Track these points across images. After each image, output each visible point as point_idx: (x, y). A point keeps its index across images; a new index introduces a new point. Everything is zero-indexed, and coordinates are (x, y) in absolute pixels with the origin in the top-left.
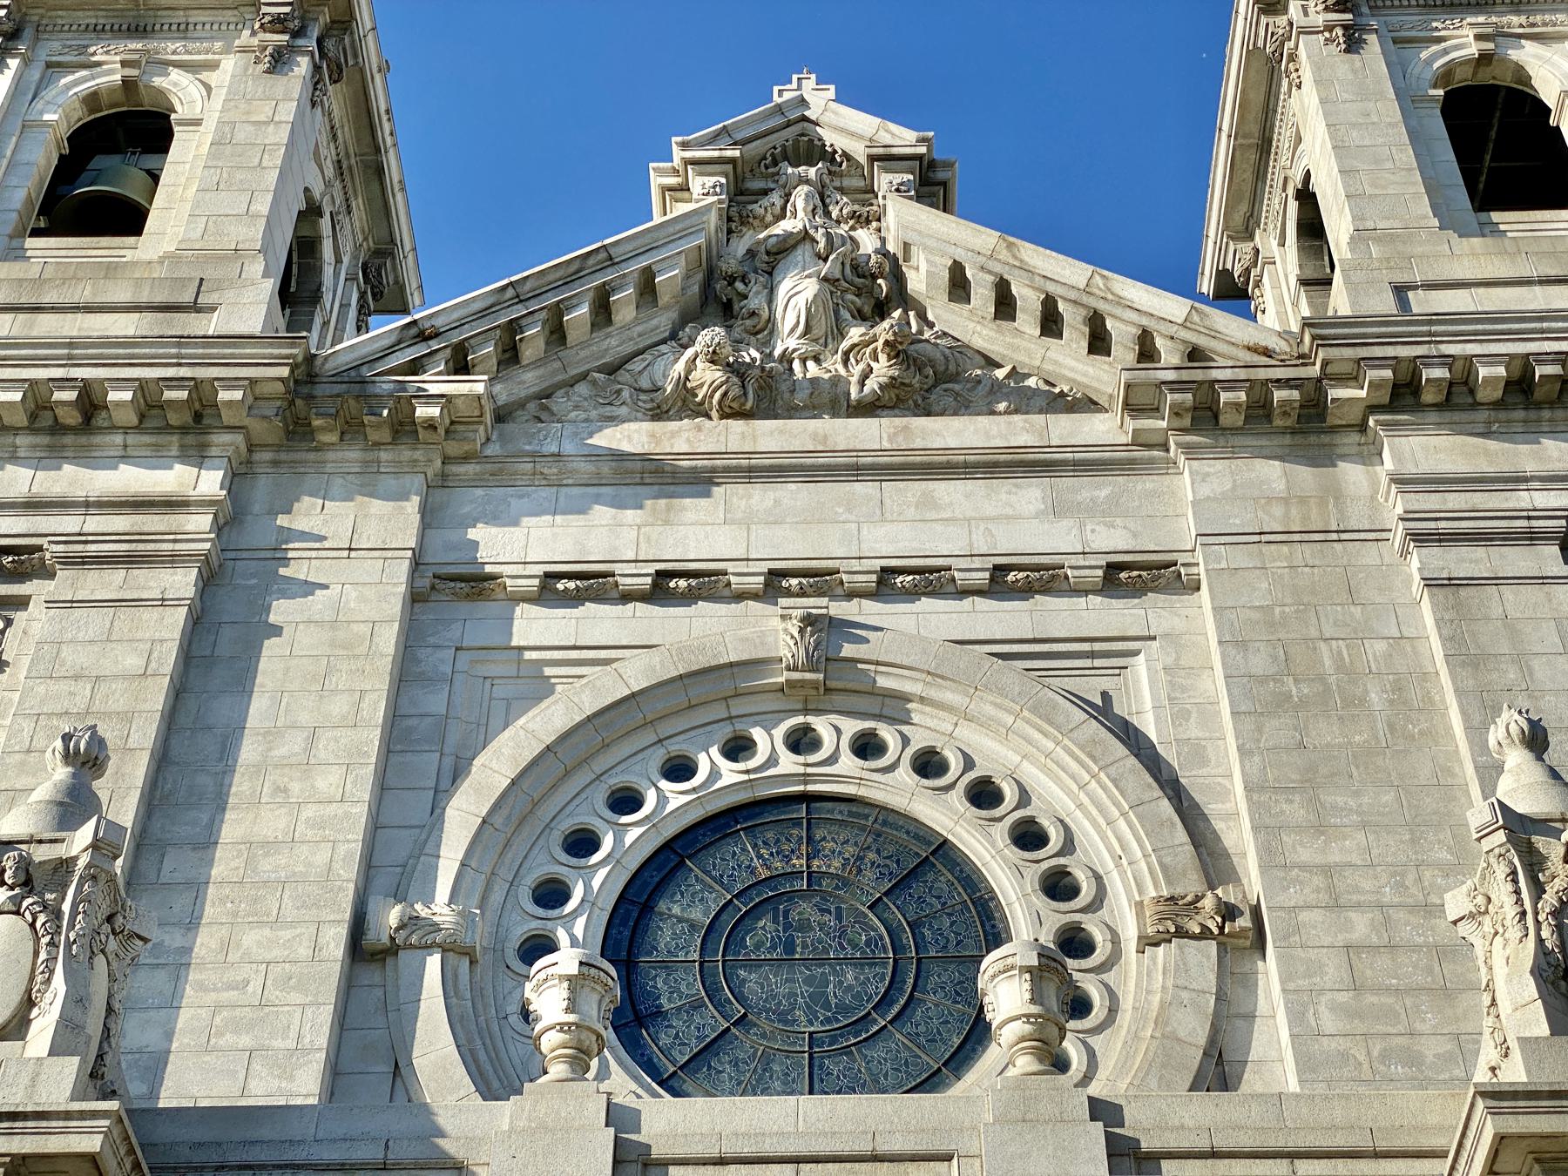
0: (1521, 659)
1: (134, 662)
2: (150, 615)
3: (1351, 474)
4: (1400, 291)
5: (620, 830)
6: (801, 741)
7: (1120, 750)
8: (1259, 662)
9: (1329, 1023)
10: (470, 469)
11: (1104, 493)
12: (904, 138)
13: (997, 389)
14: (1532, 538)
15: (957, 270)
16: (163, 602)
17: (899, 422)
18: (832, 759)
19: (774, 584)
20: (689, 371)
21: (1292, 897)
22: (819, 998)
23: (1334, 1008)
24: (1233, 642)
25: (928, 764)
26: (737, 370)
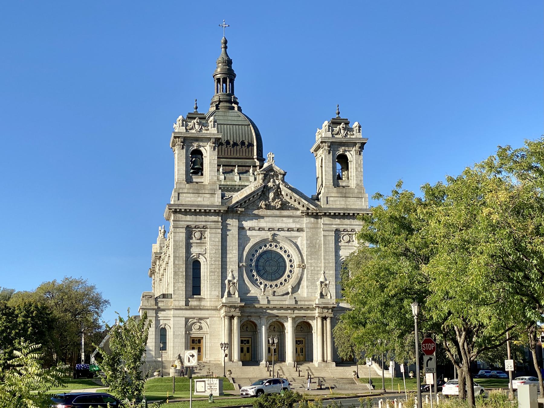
0: (329, 244)
1: (218, 240)
2: (218, 234)
3: (319, 219)
4: (327, 197)
5: (256, 254)
6: (271, 245)
7: (297, 249)
8: (309, 242)
9: (309, 276)
10: (241, 215)
11: (298, 220)
12: (282, 172)
13: (290, 207)
14: (332, 231)
15: (287, 194)
16: (219, 233)
17: (280, 211)
18: (273, 247)
19: (269, 230)
20: (262, 204)
21: (308, 265)
22: (272, 269)
23: (310, 275)
24: (307, 240)
25: (281, 248)
26: (266, 205)
